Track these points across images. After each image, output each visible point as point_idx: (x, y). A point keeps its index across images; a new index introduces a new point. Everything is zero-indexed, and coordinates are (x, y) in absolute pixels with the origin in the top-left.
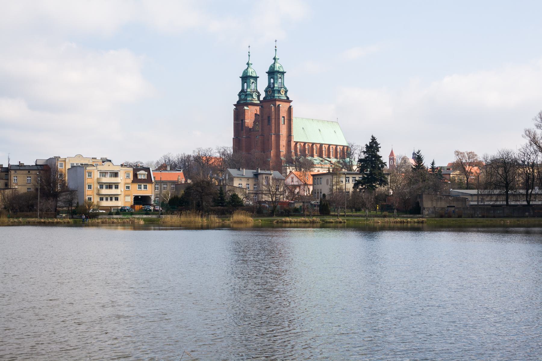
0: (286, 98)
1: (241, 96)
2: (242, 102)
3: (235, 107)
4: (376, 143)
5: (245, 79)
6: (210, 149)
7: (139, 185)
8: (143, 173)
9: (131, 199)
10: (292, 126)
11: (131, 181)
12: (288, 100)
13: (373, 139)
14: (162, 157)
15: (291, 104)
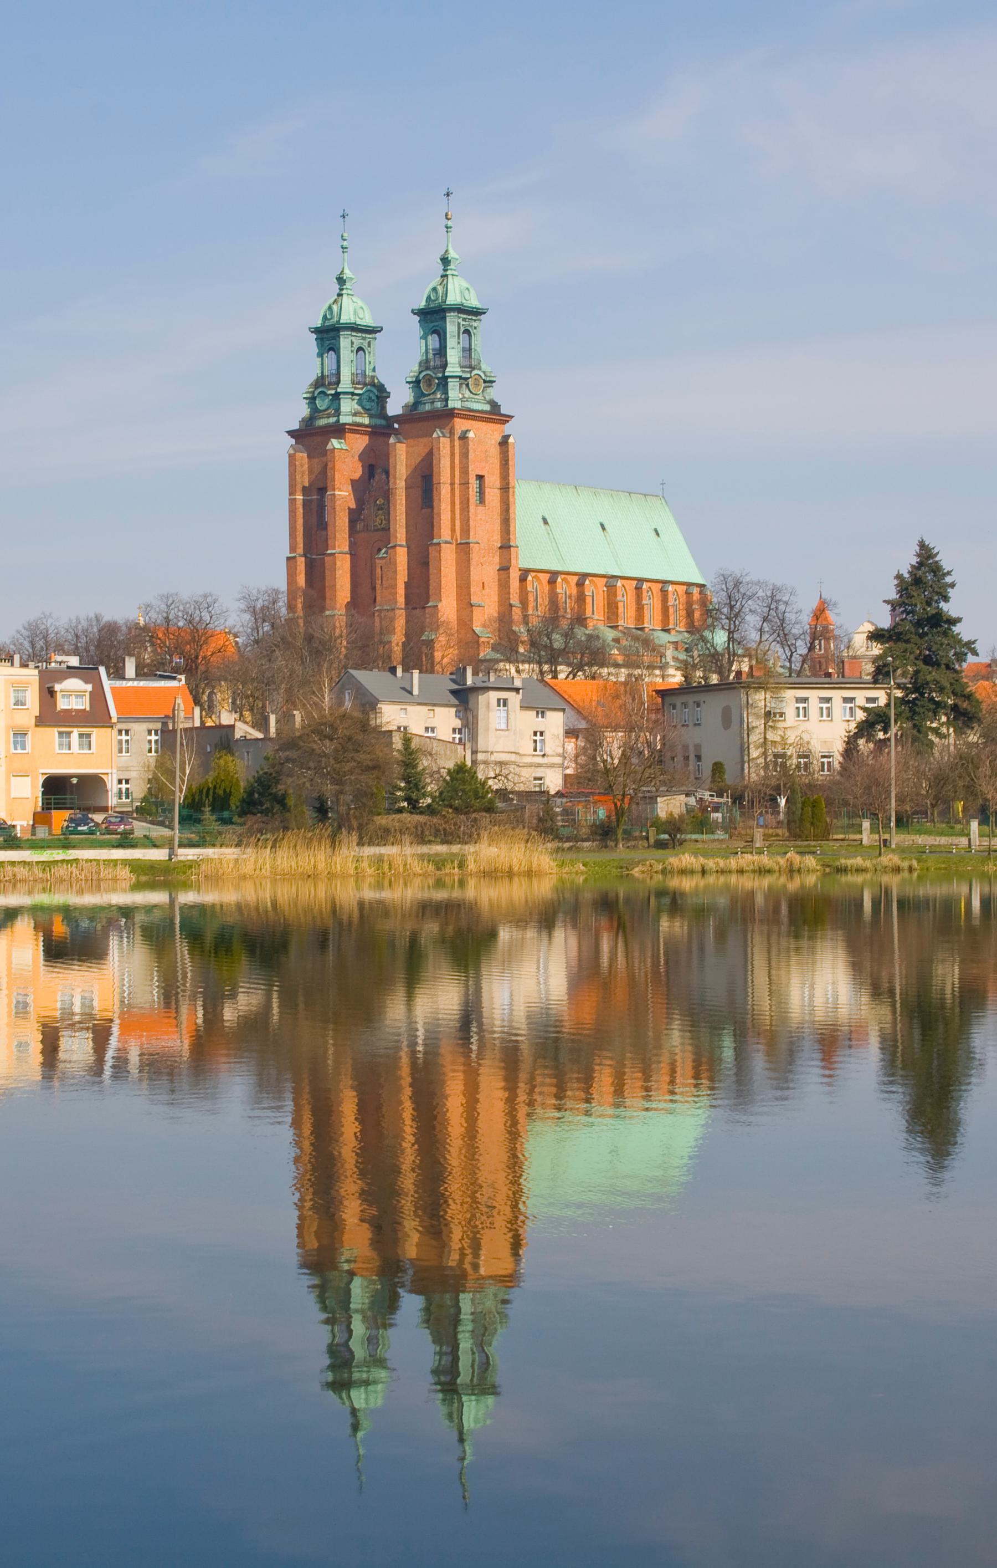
0: (487, 408)
2: (322, 422)
3: (293, 441)
4: (936, 570)
5: (332, 334)
6: (209, 599)
7: (60, 733)
8: (77, 688)
9: (33, 786)
10: (511, 511)
11: (33, 720)
12: (496, 415)
13: (926, 555)
14: (23, 631)
15: (508, 428)
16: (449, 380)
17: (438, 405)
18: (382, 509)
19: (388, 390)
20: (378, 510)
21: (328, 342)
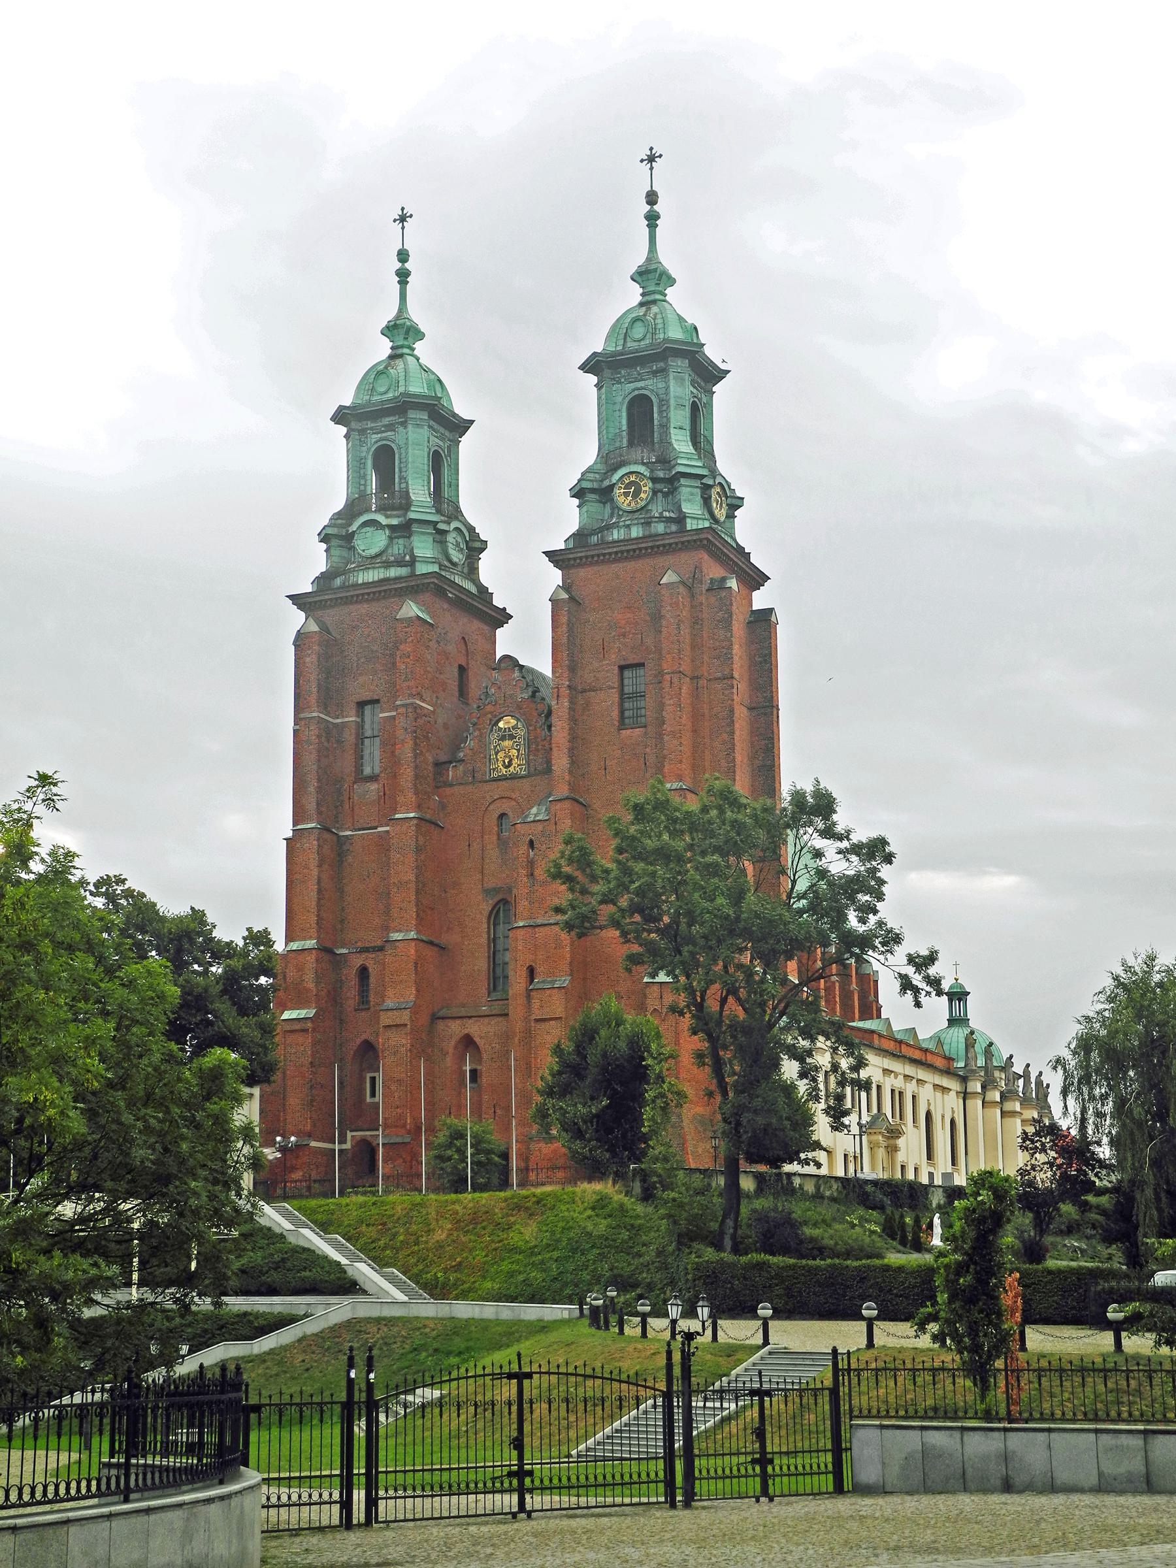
1: (350, 537)
2: (372, 576)
5: (386, 421)
16: (683, 481)
17: (660, 528)
18: (512, 737)
19: (483, 537)
20: (503, 738)
21: (376, 437)
